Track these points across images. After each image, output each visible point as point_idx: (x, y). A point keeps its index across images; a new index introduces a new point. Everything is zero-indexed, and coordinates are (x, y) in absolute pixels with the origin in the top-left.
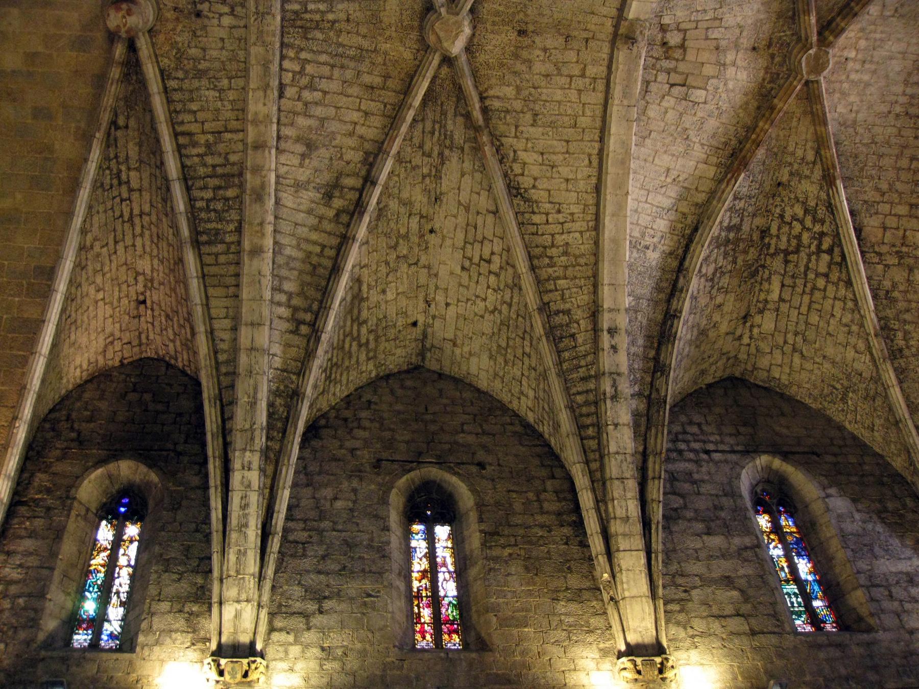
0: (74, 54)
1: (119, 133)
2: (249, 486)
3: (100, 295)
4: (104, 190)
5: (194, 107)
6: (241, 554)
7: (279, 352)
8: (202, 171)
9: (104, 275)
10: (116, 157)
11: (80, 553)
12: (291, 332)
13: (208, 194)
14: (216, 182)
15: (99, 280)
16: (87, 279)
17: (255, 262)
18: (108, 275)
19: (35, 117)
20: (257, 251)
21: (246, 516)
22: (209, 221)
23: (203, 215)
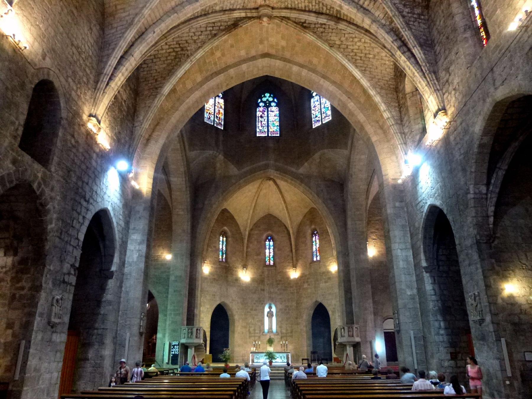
0: (282, 28)
1: (307, 22)
2: (405, 62)
3: (363, 40)
4: (324, 32)
5: (297, 3)
6: (420, 82)
7: (379, 13)
8: (317, 7)
9: (356, 37)
10: (315, 24)
11: (417, 108)
12: (374, 4)
13: (325, 8)
14: (321, 4)
15: (356, 40)
16: (353, 45)
17: (344, 8)
18: (357, 35)
19: (300, 43)
20: (341, 6)
21: (412, 71)
22: (333, 11)
23: (331, 12)
